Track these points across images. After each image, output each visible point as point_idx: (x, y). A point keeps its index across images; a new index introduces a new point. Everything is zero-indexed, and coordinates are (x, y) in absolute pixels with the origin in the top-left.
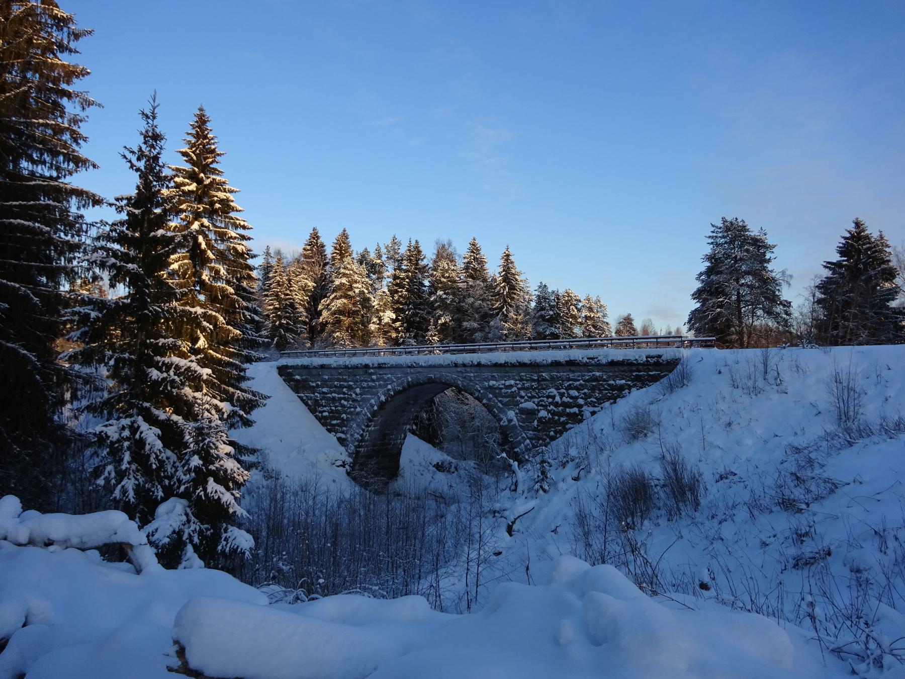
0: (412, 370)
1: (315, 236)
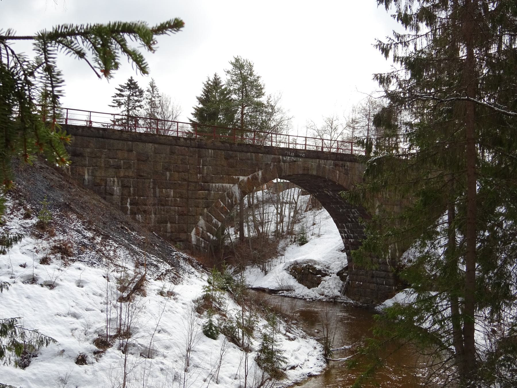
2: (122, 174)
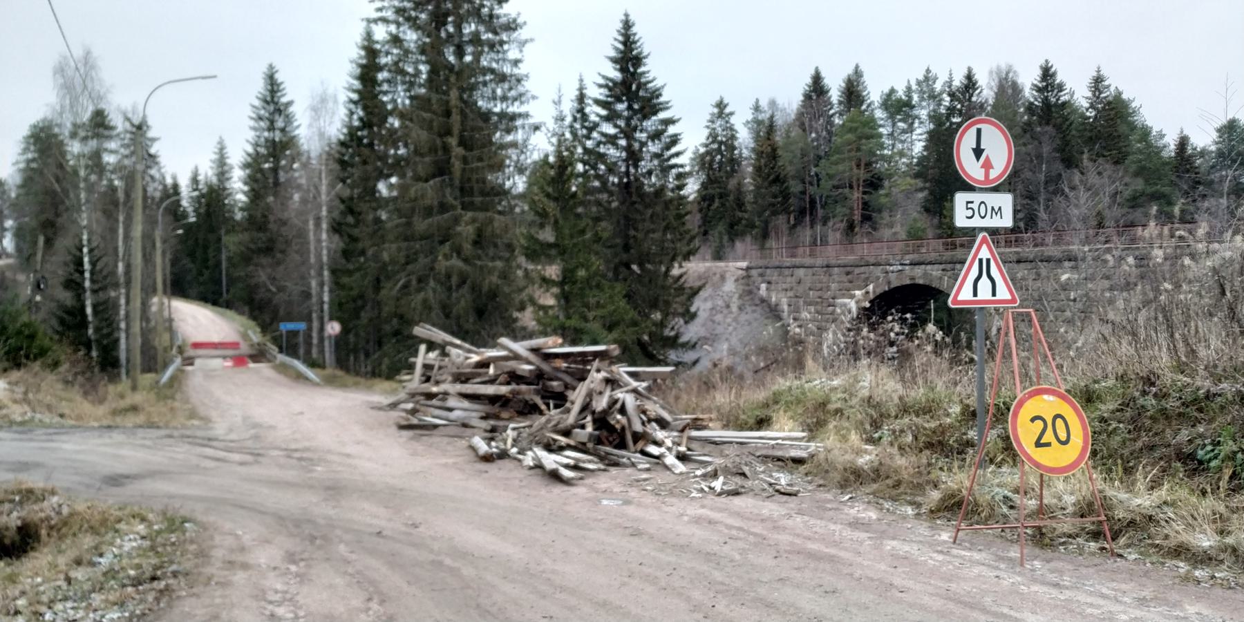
0: (891, 268)
1: (817, 79)
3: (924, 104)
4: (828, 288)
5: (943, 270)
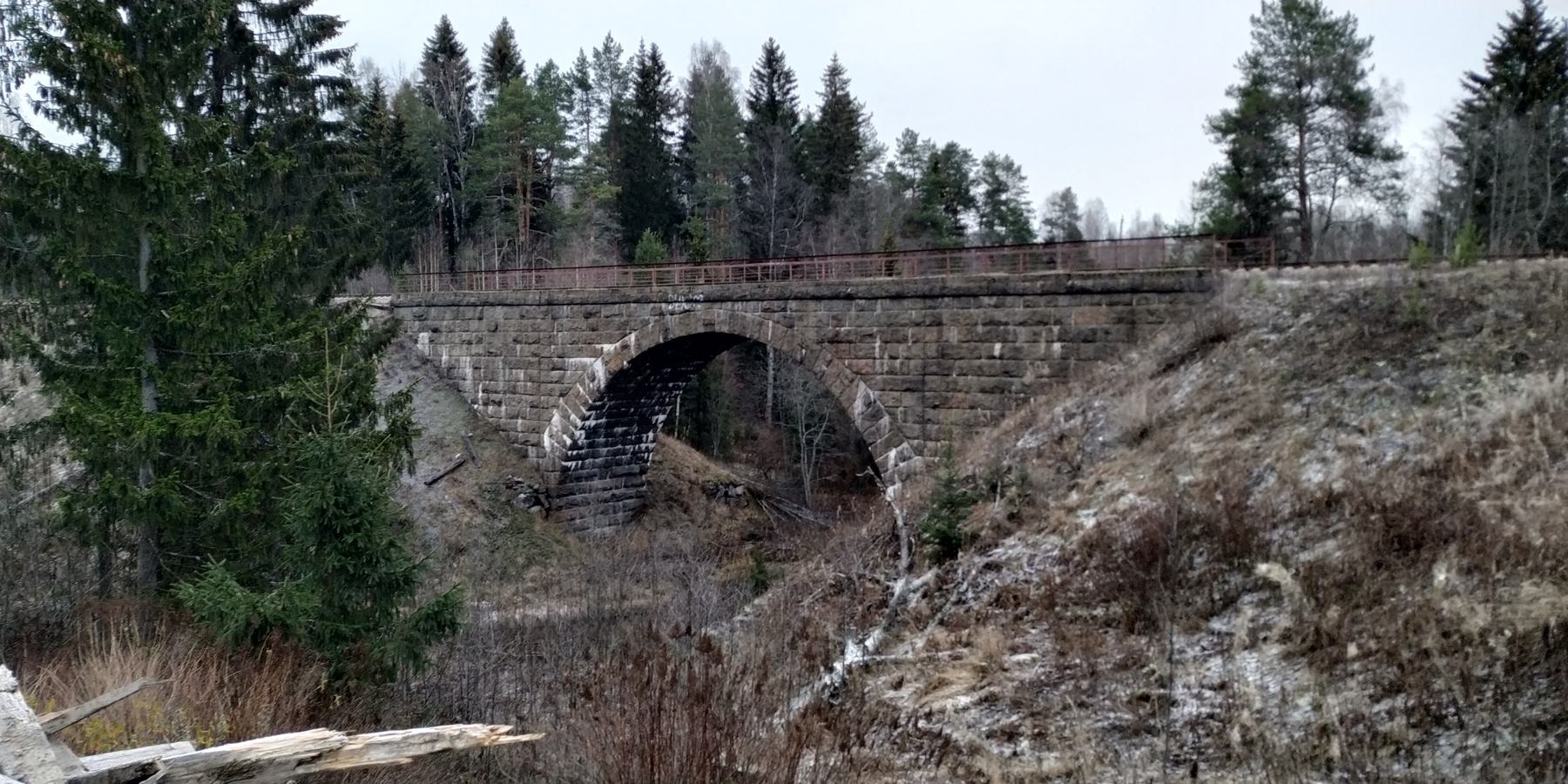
0: (670, 307)
1: (445, 32)
2: (473, 352)
3: (605, 84)
4: (551, 340)
5: (765, 310)
